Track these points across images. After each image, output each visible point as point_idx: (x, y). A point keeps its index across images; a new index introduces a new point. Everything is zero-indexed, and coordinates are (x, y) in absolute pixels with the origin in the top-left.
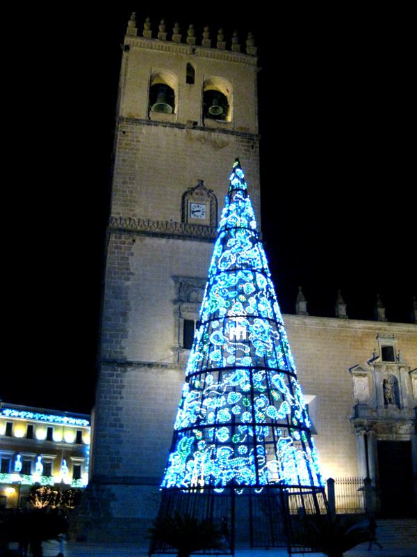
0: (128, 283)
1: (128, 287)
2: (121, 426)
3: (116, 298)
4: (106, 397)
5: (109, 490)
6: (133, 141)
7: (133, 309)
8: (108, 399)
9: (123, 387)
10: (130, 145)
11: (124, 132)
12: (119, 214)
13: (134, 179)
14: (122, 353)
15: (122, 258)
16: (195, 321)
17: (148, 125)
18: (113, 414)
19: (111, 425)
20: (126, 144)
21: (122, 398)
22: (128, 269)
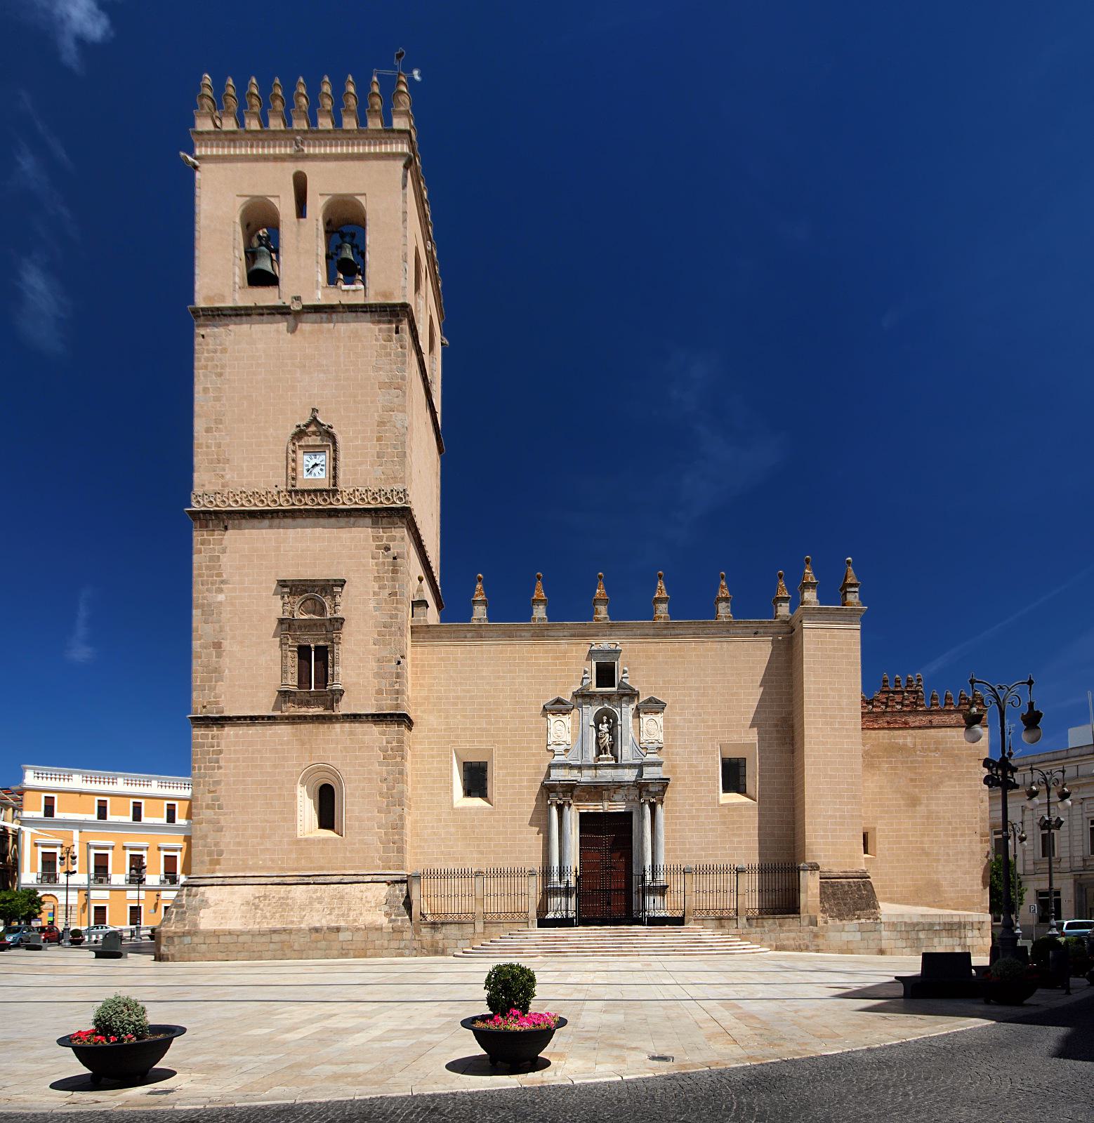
0: (221, 597)
1: (220, 603)
2: (220, 807)
3: (206, 622)
4: (200, 769)
5: (203, 894)
6: (215, 351)
7: (229, 637)
8: (202, 771)
9: (221, 752)
10: (212, 359)
11: (203, 336)
12: (203, 485)
13: (221, 422)
14: (217, 703)
15: (212, 559)
16: (312, 645)
17: (237, 315)
18: (210, 792)
19: (208, 807)
20: (207, 359)
21: (219, 768)
22: (219, 575)
